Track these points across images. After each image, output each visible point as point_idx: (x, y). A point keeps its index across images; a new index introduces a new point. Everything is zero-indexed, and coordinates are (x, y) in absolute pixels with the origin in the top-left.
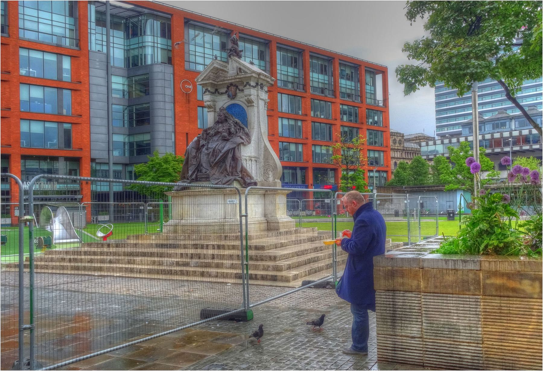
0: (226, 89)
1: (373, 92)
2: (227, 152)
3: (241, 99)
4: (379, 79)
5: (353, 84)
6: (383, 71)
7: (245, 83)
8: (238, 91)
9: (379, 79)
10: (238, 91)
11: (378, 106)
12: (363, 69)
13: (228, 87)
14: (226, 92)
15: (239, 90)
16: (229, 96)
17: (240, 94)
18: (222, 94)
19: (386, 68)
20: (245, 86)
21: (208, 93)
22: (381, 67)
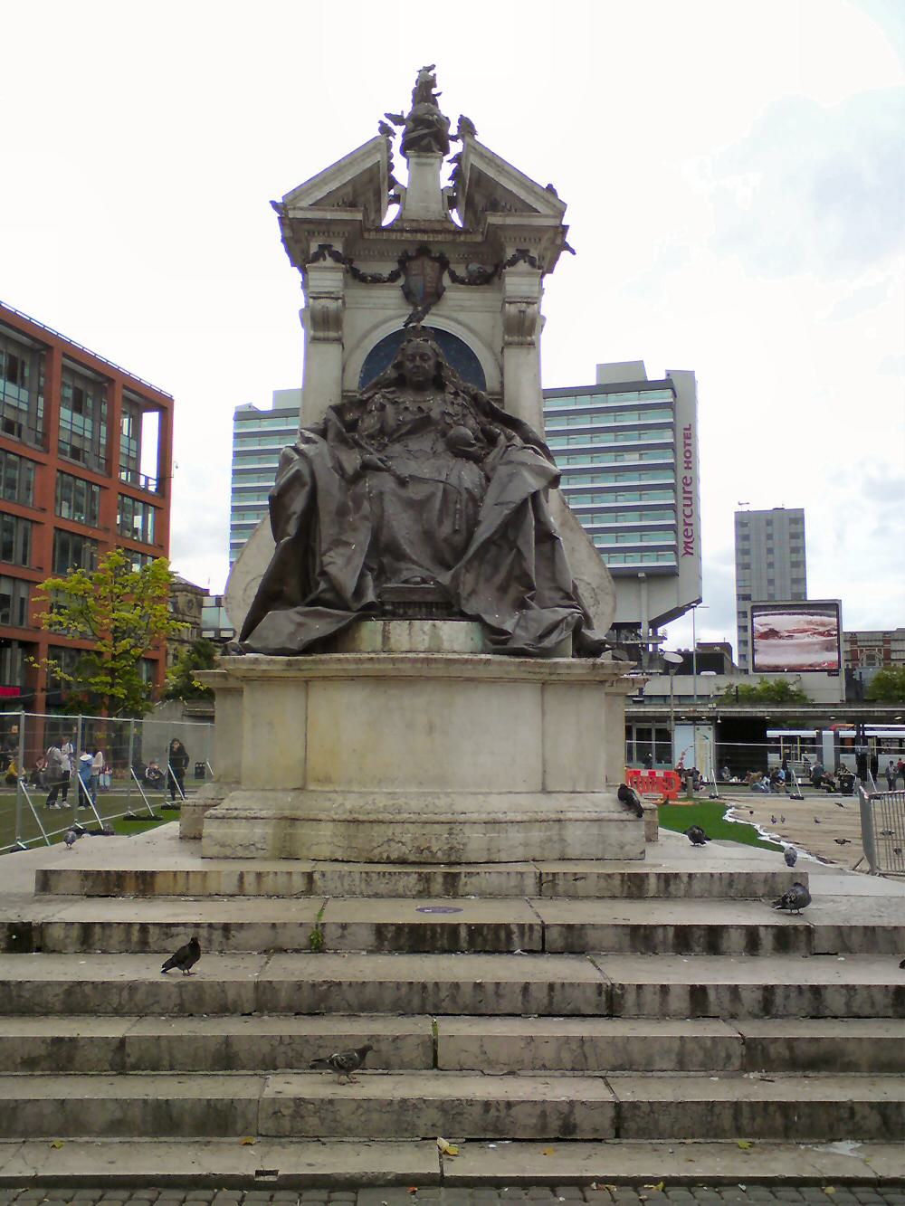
0: (394, 266)
1: (133, 455)
2: (520, 510)
3: (462, 316)
4: (151, 420)
5: (89, 422)
6: (163, 406)
7: (510, 253)
8: (446, 280)
9: (151, 420)
10: (446, 280)
11: (146, 490)
12: (120, 392)
13: (404, 261)
14: (393, 277)
15: (454, 278)
16: (408, 295)
17: (456, 297)
18: (377, 280)
19: (170, 400)
20: (513, 262)
21: (329, 262)
22: (159, 394)
